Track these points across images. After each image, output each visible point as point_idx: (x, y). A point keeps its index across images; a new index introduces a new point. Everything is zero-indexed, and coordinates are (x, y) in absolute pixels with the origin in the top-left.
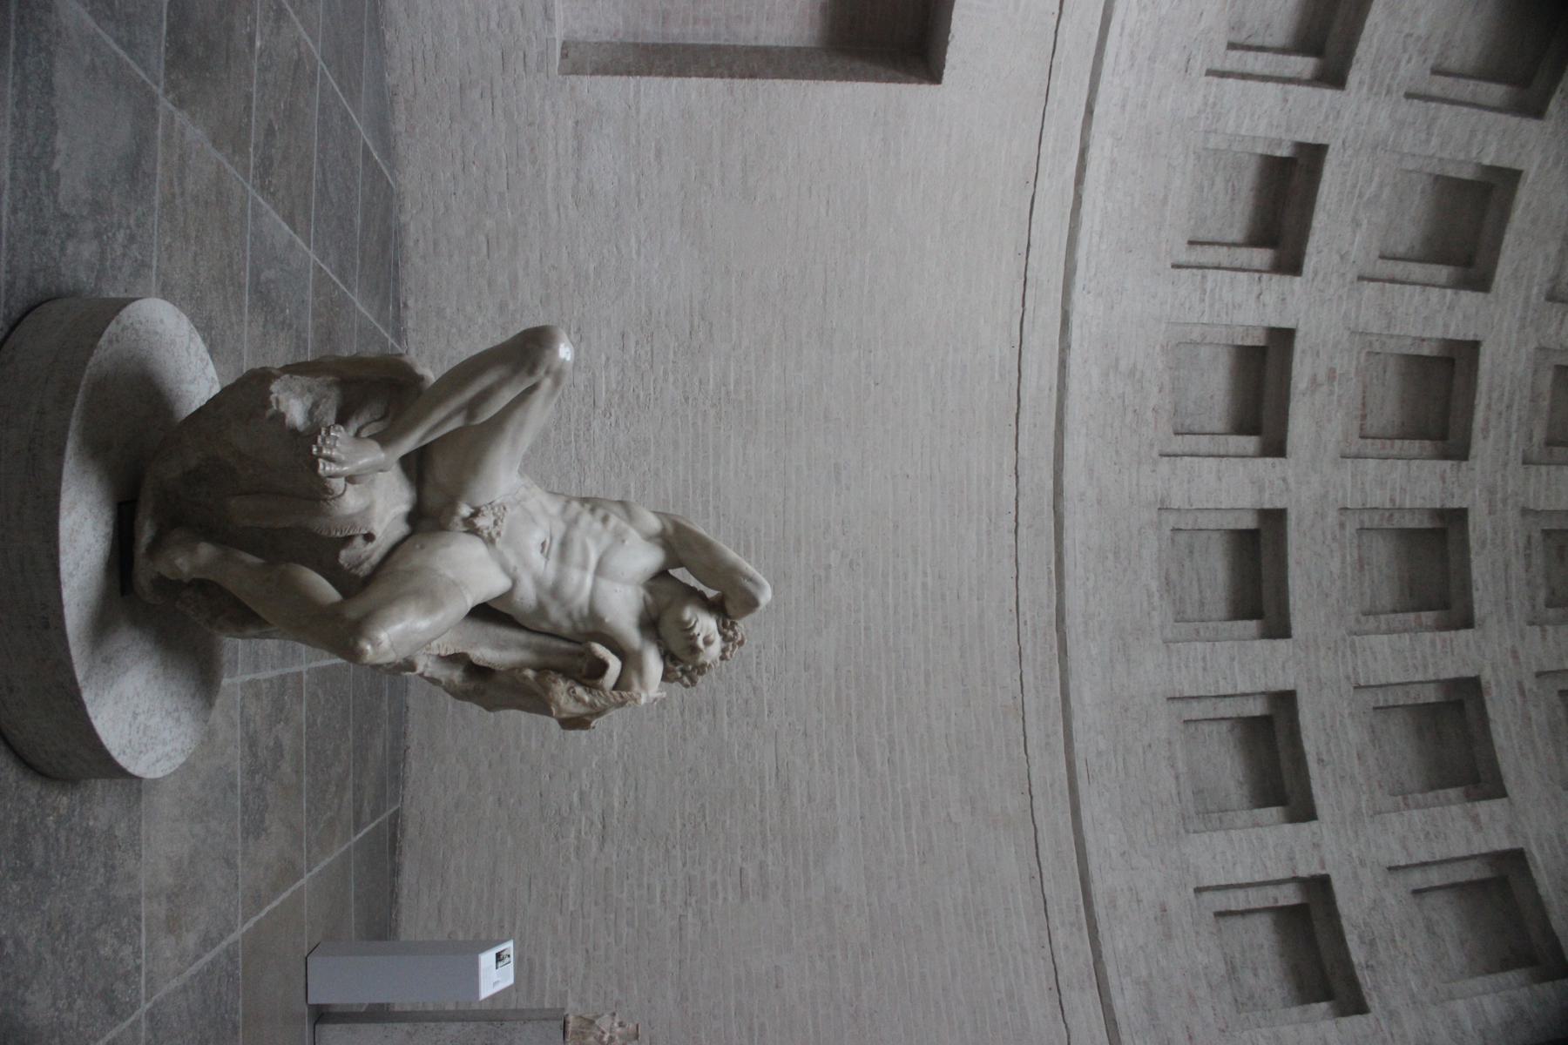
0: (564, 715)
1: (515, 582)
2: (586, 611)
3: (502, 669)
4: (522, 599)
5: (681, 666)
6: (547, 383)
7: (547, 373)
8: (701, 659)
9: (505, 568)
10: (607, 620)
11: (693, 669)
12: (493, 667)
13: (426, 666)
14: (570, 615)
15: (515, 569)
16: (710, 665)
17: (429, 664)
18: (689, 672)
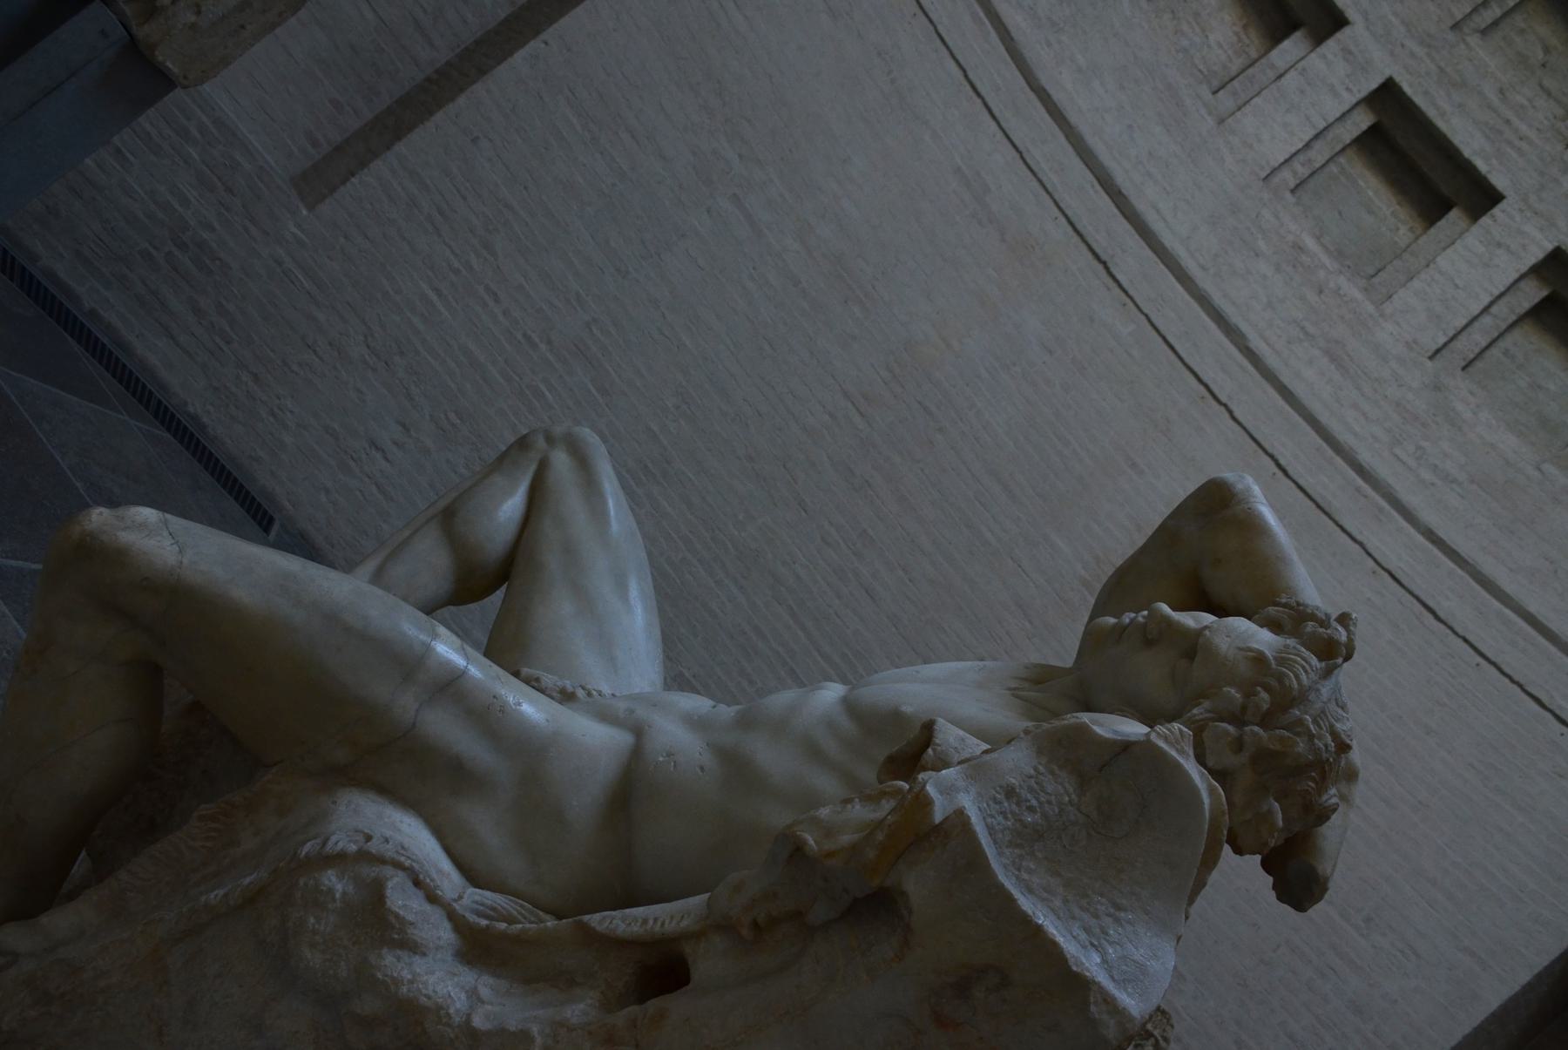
0: (846, 839)
1: (639, 731)
2: (846, 724)
3: (684, 923)
4: (669, 754)
5: (1207, 704)
6: (561, 461)
7: (550, 440)
8: (1223, 644)
9: (605, 716)
10: (908, 709)
11: (1249, 694)
12: (657, 928)
13: (473, 994)
14: (814, 753)
15: (632, 712)
16: (1281, 661)
17: (484, 992)
18: (1244, 708)
